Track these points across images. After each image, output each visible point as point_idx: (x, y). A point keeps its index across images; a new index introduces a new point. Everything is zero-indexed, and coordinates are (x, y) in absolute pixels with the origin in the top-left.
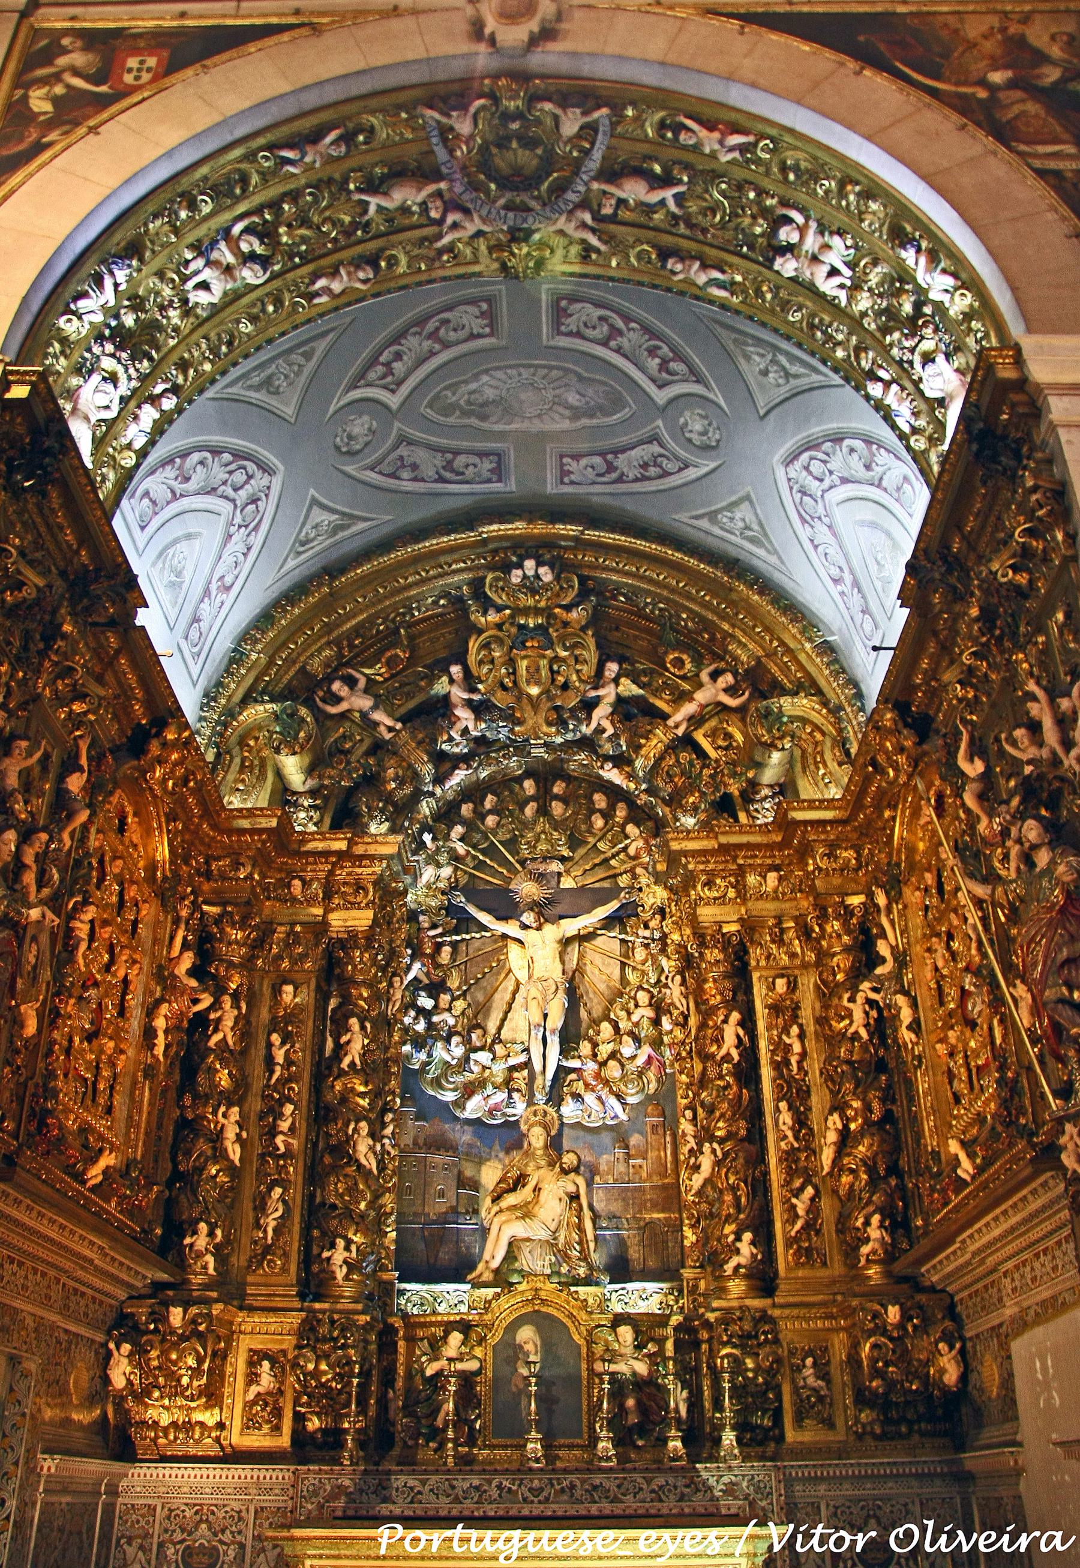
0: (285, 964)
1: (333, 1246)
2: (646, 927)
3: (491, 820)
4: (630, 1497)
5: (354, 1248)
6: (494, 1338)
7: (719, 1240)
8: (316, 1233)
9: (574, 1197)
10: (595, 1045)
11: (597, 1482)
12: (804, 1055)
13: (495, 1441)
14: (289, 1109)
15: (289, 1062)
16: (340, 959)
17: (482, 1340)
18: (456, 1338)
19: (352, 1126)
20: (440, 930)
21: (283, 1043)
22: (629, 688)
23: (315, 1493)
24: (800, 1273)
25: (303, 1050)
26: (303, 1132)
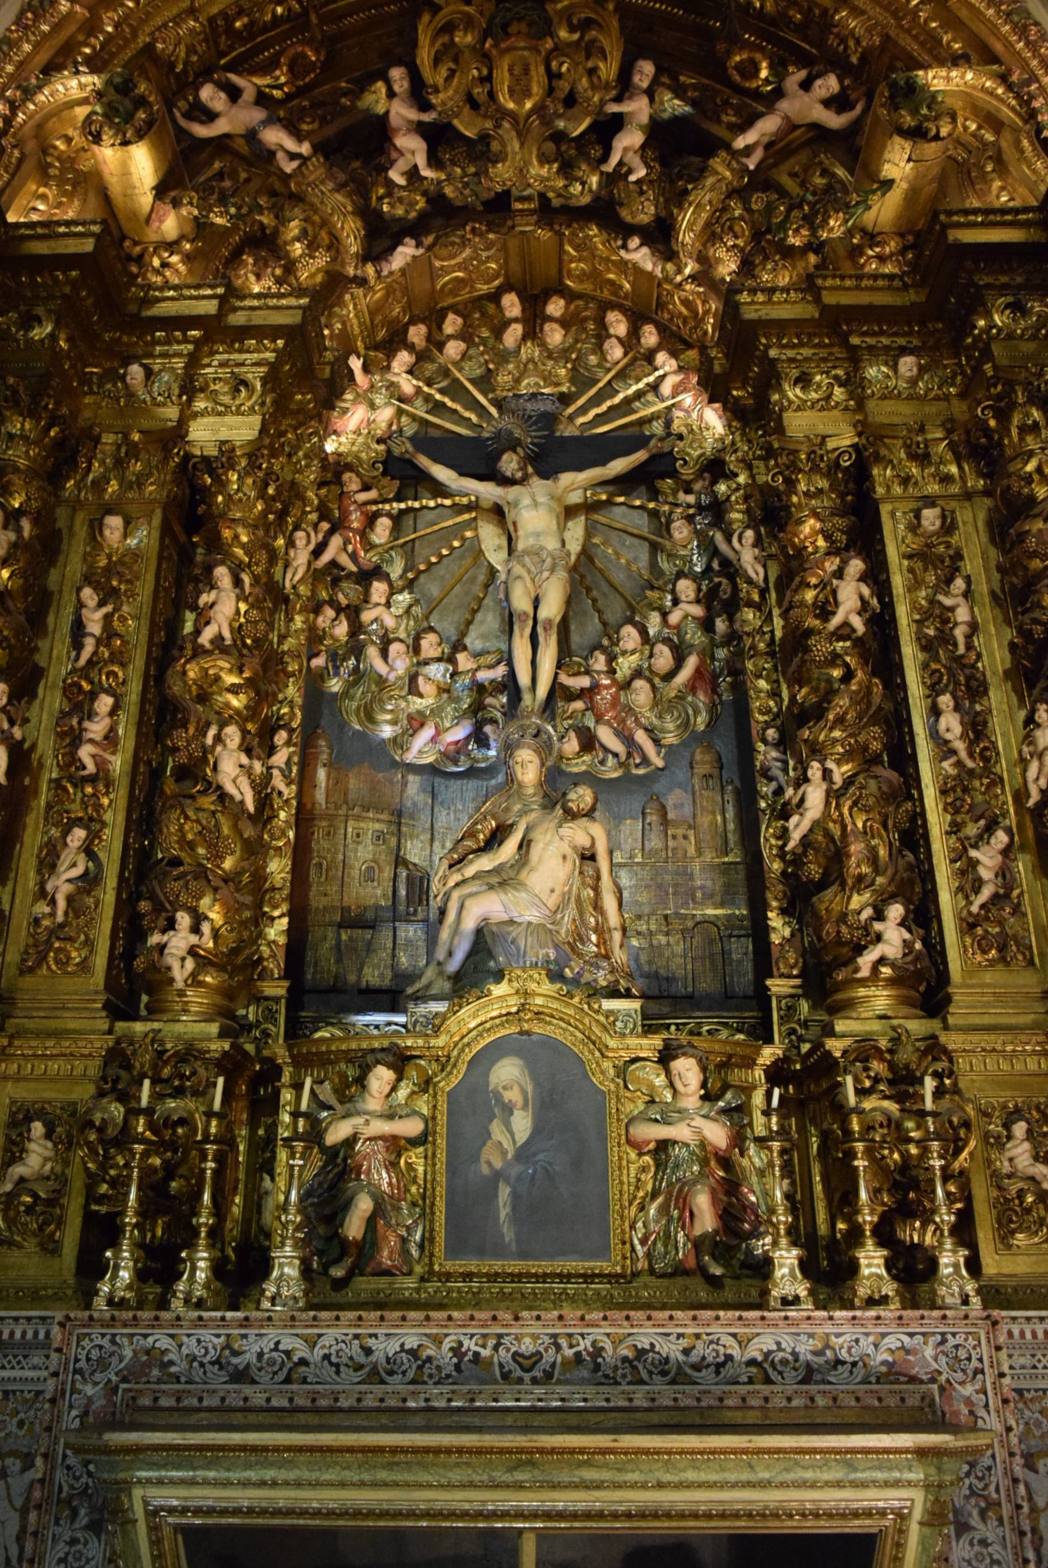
0: (113, 487)
1: (171, 925)
2: (688, 491)
3: (454, 349)
4: (708, 1374)
5: (206, 928)
6: (448, 1083)
7: (843, 917)
8: (144, 906)
9: (588, 857)
10: (611, 658)
11: (644, 1343)
12: (974, 627)
13: (450, 1266)
14: (105, 702)
15: (109, 633)
16: (205, 489)
17: (426, 1084)
18: (381, 1077)
19: (212, 732)
20: (373, 494)
21: (101, 604)
22: (673, 105)
23: (103, 1364)
24: (988, 977)
25: (136, 618)
26: (130, 744)
